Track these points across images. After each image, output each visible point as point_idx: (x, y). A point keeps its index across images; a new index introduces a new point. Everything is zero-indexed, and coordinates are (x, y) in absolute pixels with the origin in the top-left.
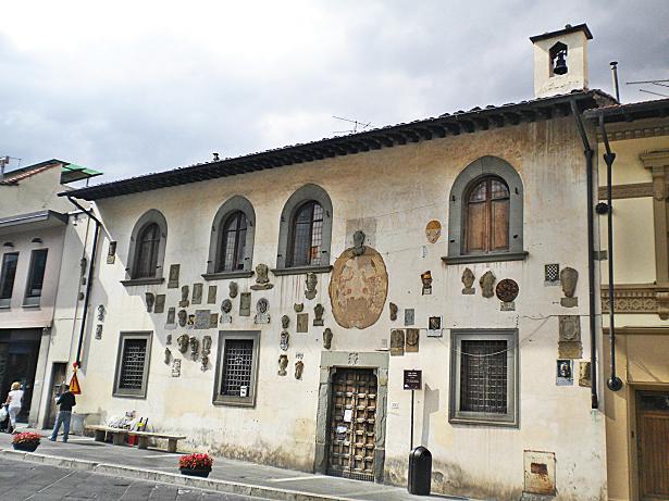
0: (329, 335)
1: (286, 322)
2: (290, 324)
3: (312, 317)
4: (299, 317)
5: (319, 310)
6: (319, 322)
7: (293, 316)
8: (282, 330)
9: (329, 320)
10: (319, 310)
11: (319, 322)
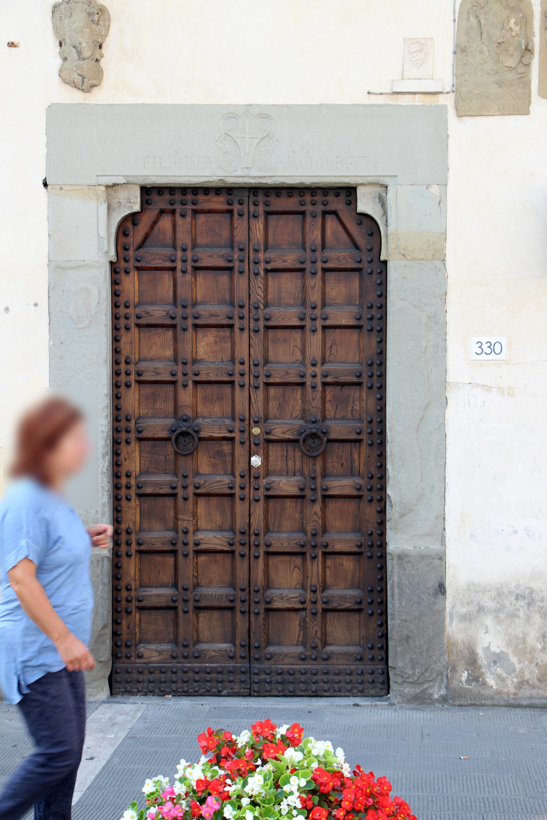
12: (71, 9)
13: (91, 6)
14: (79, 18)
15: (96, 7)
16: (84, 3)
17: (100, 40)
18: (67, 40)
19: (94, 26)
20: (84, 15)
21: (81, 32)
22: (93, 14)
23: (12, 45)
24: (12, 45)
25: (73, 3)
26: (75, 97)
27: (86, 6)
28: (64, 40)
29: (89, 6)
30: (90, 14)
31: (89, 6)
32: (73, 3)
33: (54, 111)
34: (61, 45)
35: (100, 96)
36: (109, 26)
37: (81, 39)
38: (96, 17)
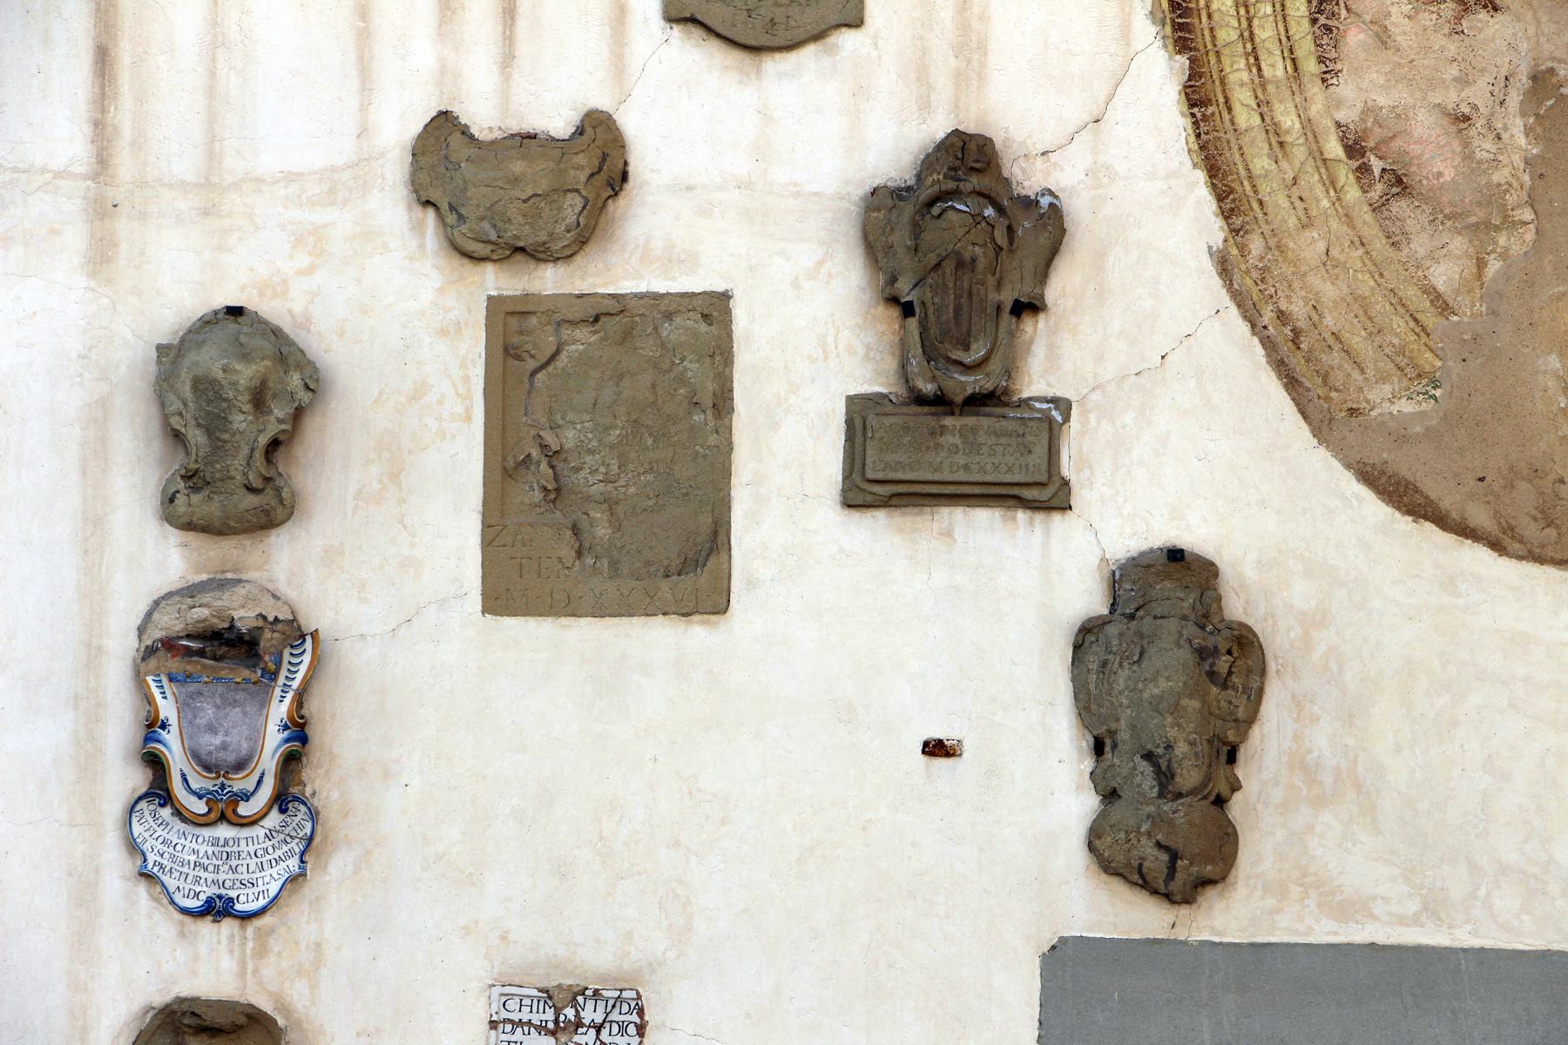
0: (1174, 687)
1: (235, 422)
2: (336, 469)
3: (811, 352)
4: (518, 349)
5: (961, 247)
6: (956, 412)
7: (405, 341)
8: (156, 563)
9: (1171, 415)
10: (961, 247)
11: (956, 412)
12: (1142, 636)
13: (1209, 628)
14: (1169, 667)
15: (1227, 633)
16: (1184, 618)
17: (1231, 736)
18: (1124, 735)
19: (1214, 690)
20: (1185, 654)
21: (1176, 709)
22: (1215, 652)
23: (936, 749)
24: (936, 749)
25: (1148, 620)
26: (1137, 917)
27: (1191, 630)
28: (1112, 733)
29: (1203, 628)
30: (1203, 654)
31: (1203, 628)
32: (1148, 620)
33: (1069, 966)
34: (1099, 748)
35: (1226, 919)
36: (1261, 691)
37: (1172, 733)
38: (1223, 664)
